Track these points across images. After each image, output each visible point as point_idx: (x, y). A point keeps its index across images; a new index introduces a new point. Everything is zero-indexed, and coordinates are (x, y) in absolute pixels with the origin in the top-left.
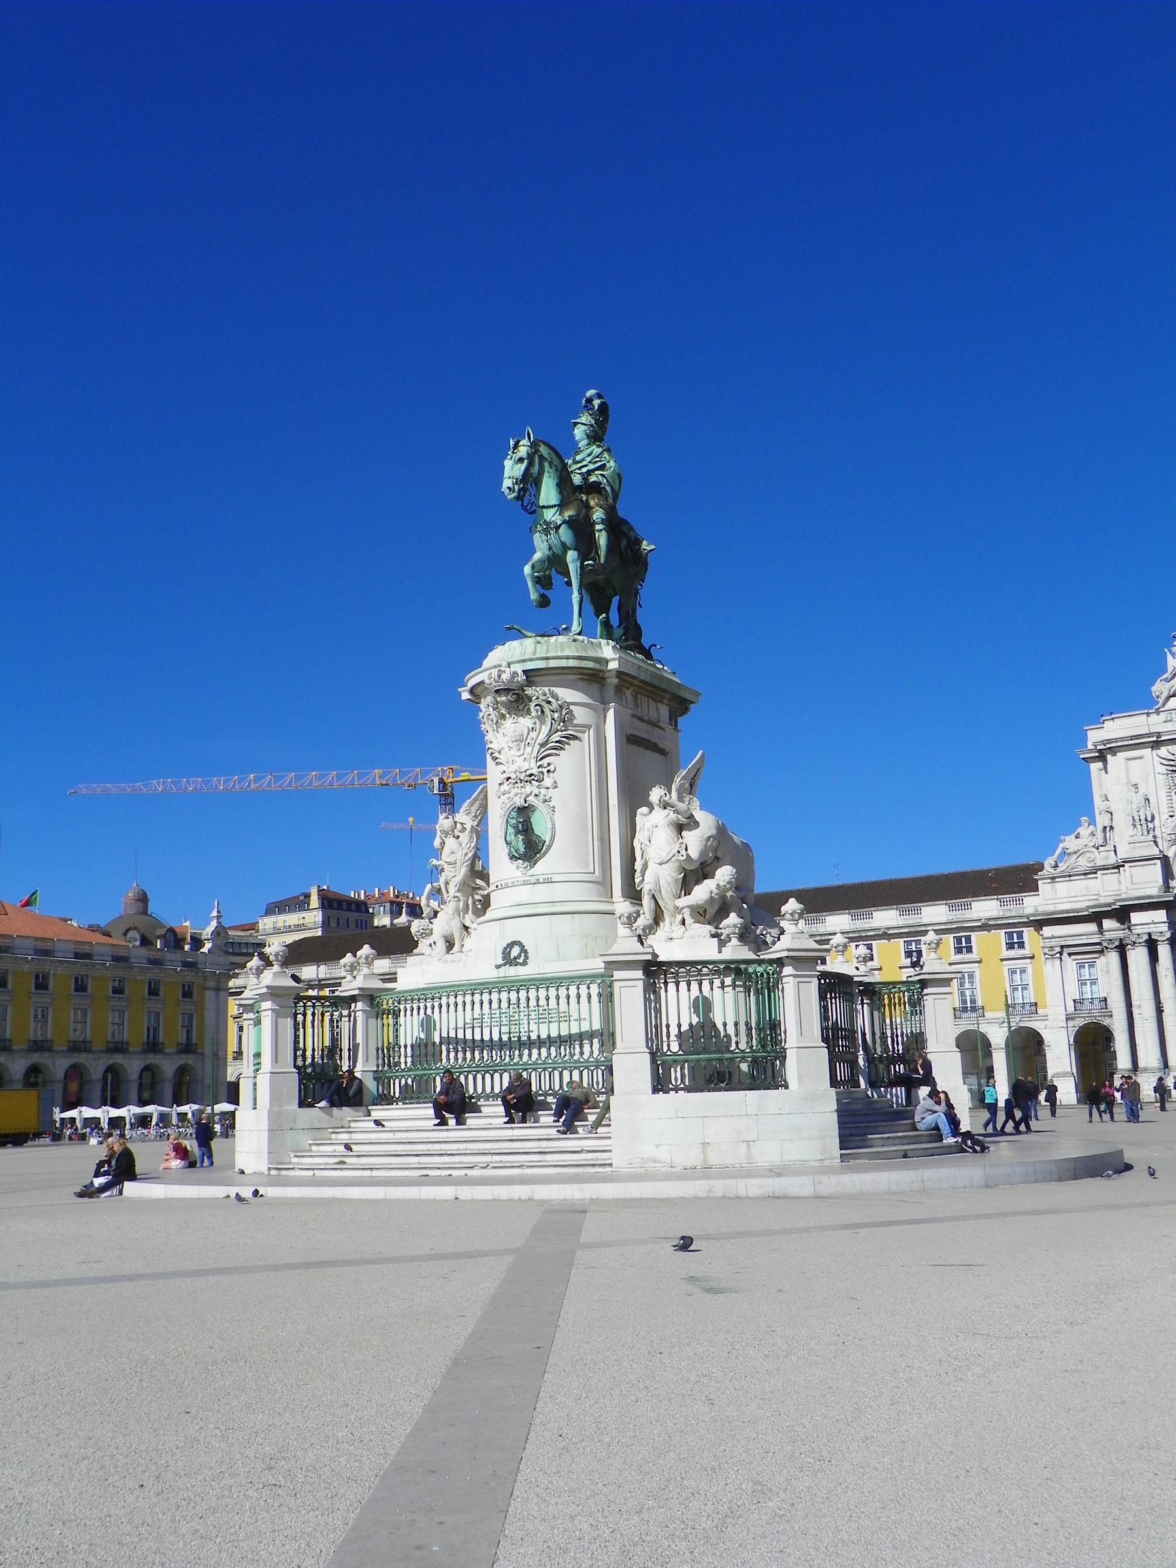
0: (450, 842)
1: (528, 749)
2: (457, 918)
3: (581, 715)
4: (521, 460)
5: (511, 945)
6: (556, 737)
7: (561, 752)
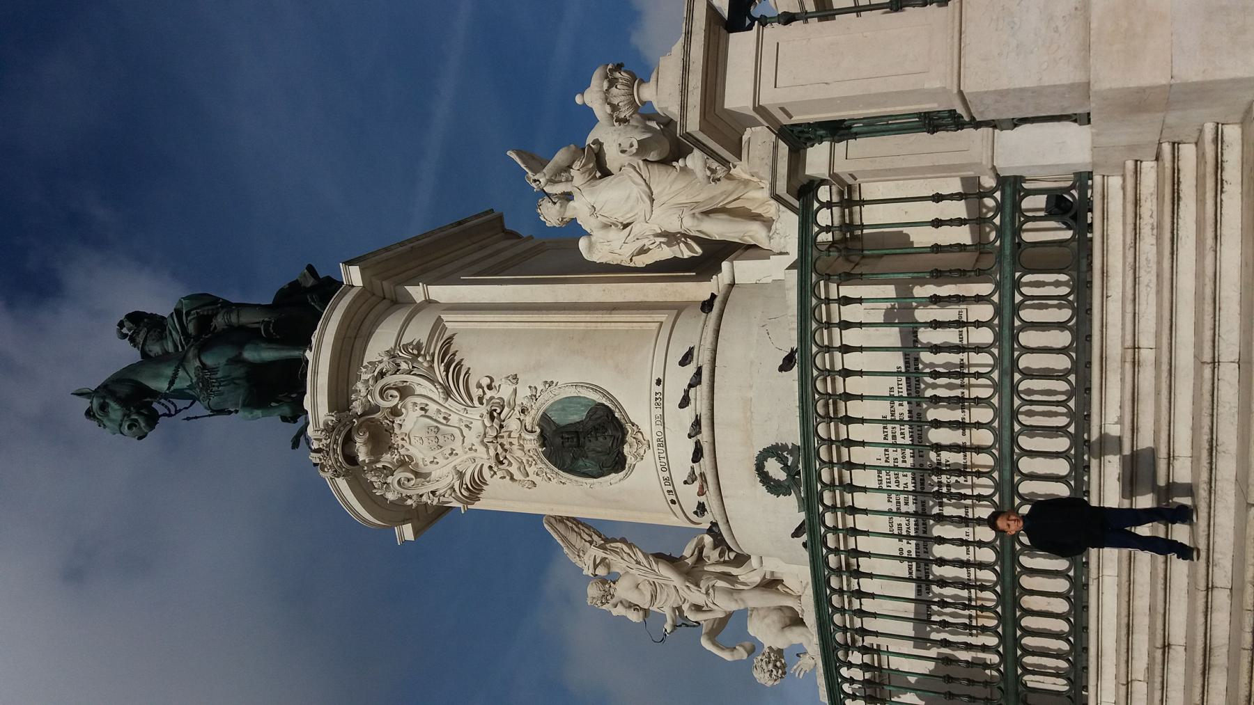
0: (622, 590)
1: (454, 419)
3: (419, 331)
5: (760, 469)
7: (466, 364)
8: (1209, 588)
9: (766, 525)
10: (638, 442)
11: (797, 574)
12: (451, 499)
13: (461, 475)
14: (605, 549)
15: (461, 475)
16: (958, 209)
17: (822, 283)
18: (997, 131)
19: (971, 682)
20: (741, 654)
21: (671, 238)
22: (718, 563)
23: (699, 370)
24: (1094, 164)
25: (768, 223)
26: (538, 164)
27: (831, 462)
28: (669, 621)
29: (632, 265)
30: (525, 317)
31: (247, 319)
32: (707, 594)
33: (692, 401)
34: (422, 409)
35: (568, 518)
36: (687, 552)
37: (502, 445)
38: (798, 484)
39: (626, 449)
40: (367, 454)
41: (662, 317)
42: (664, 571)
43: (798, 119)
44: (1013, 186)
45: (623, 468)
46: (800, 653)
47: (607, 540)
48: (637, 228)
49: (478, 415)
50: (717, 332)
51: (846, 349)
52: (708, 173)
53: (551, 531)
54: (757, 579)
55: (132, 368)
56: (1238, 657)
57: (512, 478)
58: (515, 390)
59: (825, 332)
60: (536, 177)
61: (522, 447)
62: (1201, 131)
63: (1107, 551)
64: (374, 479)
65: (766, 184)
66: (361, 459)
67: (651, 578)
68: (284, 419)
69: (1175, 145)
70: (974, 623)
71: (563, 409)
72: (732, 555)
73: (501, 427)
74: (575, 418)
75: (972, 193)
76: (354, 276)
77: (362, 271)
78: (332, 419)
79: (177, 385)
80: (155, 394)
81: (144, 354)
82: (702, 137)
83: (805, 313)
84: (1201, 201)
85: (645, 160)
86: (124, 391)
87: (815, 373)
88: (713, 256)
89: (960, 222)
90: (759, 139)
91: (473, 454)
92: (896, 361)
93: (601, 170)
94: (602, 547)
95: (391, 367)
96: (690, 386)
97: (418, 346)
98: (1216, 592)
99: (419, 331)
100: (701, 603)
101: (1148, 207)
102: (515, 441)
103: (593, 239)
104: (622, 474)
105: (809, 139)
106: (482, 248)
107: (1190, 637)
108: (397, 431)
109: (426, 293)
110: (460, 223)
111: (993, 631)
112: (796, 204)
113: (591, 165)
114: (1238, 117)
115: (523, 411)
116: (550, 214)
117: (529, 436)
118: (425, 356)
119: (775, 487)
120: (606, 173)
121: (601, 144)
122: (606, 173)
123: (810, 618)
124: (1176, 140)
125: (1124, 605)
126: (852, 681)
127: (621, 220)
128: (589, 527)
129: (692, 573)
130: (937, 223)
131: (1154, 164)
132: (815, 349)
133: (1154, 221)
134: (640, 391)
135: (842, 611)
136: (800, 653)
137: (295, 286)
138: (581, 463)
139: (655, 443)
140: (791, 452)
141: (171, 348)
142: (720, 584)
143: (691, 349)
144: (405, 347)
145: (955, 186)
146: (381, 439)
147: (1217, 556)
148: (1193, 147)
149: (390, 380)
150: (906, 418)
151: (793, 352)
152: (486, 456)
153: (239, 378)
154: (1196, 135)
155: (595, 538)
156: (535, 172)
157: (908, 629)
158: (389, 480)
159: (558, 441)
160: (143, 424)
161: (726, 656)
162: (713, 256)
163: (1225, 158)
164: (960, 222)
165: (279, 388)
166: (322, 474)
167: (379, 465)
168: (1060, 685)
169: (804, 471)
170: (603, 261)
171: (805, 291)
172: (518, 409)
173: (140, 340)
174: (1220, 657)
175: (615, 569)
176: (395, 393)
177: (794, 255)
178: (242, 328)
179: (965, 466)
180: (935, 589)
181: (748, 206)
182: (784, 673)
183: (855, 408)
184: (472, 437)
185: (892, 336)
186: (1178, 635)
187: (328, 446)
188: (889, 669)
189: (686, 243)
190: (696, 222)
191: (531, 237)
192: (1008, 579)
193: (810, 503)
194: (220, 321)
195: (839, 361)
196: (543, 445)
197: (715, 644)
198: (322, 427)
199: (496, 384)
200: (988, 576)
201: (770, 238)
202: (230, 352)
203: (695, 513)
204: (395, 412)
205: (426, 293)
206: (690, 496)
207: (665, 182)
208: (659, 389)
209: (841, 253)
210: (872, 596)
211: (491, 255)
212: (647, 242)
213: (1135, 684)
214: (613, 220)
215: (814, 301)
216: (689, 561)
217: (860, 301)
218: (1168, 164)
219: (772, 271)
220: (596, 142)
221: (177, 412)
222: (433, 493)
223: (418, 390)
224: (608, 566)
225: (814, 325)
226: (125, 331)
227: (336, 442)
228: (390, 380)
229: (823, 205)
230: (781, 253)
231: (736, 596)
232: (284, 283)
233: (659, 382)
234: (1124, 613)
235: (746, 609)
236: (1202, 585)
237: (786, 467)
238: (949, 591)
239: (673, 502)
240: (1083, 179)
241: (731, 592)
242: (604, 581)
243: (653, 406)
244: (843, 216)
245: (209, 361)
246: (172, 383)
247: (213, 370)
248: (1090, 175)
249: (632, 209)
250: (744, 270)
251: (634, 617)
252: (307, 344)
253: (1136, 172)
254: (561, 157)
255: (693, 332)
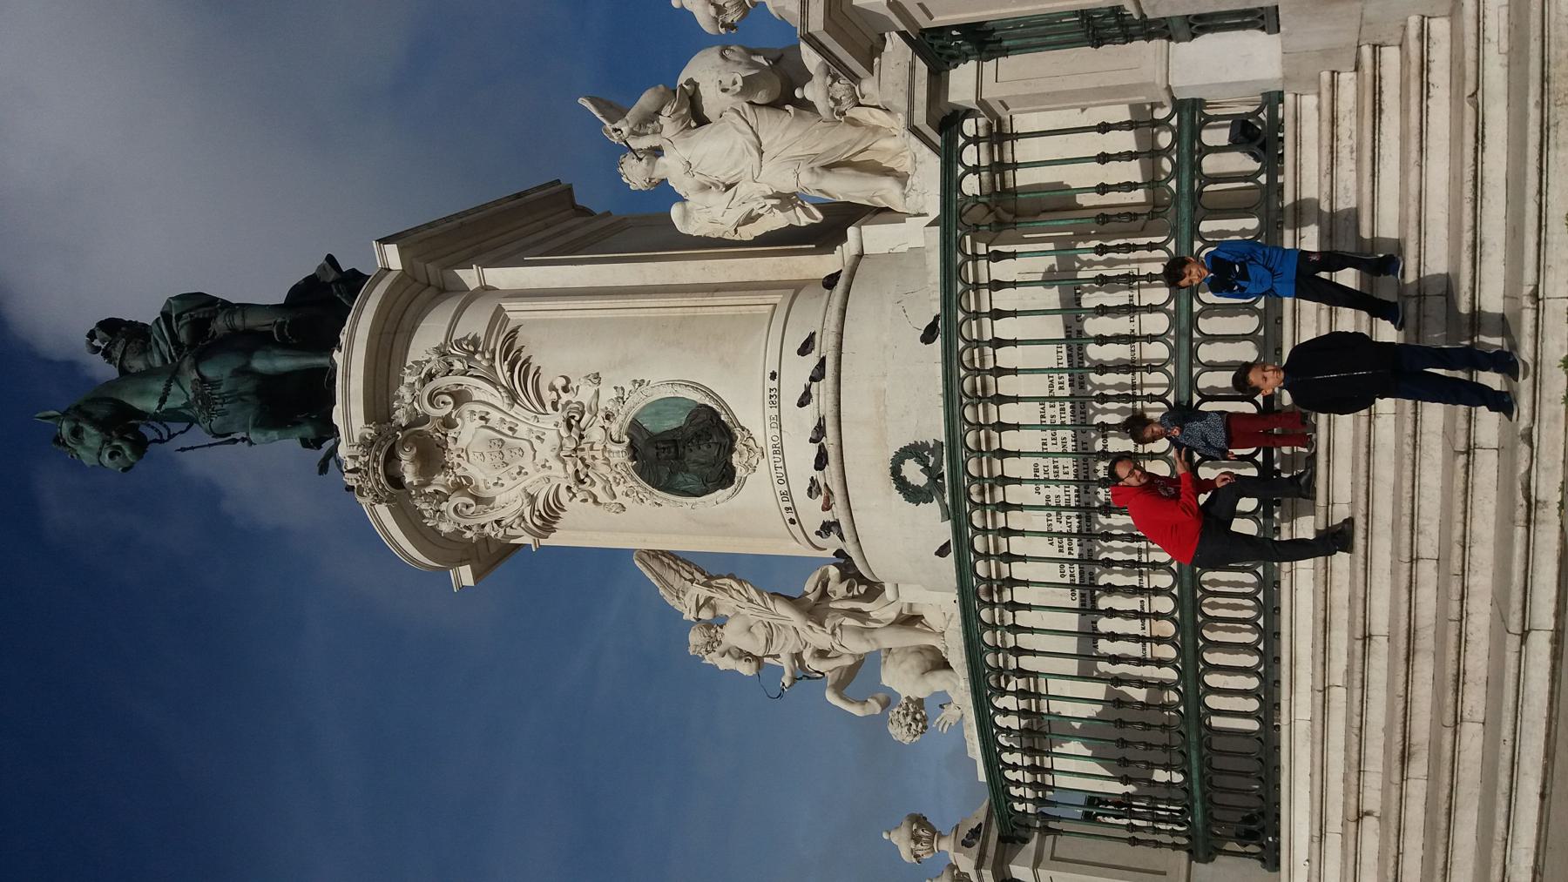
0: (732, 635)
1: (522, 430)
2: (877, 634)
4: (76, 432)
5: (896, 472)
6: (502, 371)
7: (535, 363)
8: (1414, 560)
9: (905, 543)
10: (750, 449)
11: (941, 607)
12: (520, 531)
13: (532, 499)
14: (710, 586)
15: (532, 499)
16: (1125, 141)
17: (968, 238)
18: (1172, 44)
19: (1147, 726)
20: (874, 707)
21: (786, 200)
22: (845, 598)
23: (823, 361)
24: (1286, 79)
25: (902, 179)
26: (615, 111)
27: (981, 477)
28: (788, 673)
29: (737, 238)
30: (606, 303)
31: (252, 321)
32: (833, 634)
33: (815, 397)
34: (482, 418)
35: (664, 553)
36: (809, 587)
37: (583, 460)
38: (941, 489)
39: (735, 458)
40: (415, 474)
41: (776, 298)
42: (782, 609)
43: (940, 20)
44: (1192, 112)
45: (732, 483)
46: (943, 701)
47: (710, 578)
48: (743, 189)
49: (551, 423)
50: (843, 312)
51: (997, 314)
52: (832, 104)
53: (643, 569)
54: (893, 615)
55: (110, 384)
56: (1445, 629)
57: (595, 501)
58: (597, 392)
59: (972, 293)
60: (616, 126)
61: (607, 461)
62: (1405, 28)
63: (1301, 564)
64: (424, 506)
65: (902, 118)
66: (407, 480)
67: (766, 618)
68: (305, 443)
69: (1376, 48)
70: (1144, 559)
71: (657, 413)
72: (863, 589)
73: (581, 437)
74: (671, 424)
75: (1142, 122)
76: (393, 257)
77: (401, 250)
78: (370, 432)
79: (169, 404)
80: (142, 415)
81: (123, 371)
82: (826, 39)
83: (950, 272)
84: (1404, 111)
85: (751, 103)
86: (102, 411)
87: (963, 373)
88: (837, 221)
89: (1130, 156)
90: (896, 50)
91: (546, 472)
92: (1054, 327)
93: (697, 117)
94: (707, 585)
95: (442, 366)
96: (812, 379)
97: (475, 341)
98: (1421, 564)
99: (474, 323)
100: (826, 646)
101: (1346, 126)
102: (599, 455)
103: (689, 205)
104: (730, 490)
105: (952, 57)
106: (547, 227)
107: (1393, 623)
108: (451, 446)
109: (481, 278)
110: (518, 196)
111: (1165, 567)
112: (937, 140)
113: (684, 111)
114: (1445, 8)
115: (607, 417)
116: (635, 174)
117: (615, 448)
118: (483, 353)
119: (913, 494)
120: (702, 121)
121: (696, 85)
122: (702, 121)
123: (957, 658)
124: (1377, 41)
125: (1321, 597)
126: (1008, 730)
127: (722, 179)
128: (689, 564)
129: (815, 610)
130: (1103, 158)
131: (1353, 75)
132: (961, 316)
133: (1354, 142)
134: (750, 386)
135: (993, 627)
136: (943, 701)
137: (311, 281)
138: (680, 478)
139: (770, 450)
140: (932, 452)
141: (157, 362)
142: (849, 622)
143: (812, 335)
144: (459, 343)
145: (1122, 114)
146: (432, 456)
147: (1422, 522)
148: (1397, 49)
149: (441, 382)
150: (1065, 365)
151: (937, 318)
152: (562, 474)
153: (246, 393)
154: (1399, 34)
155: (697, 575)
156: (613, 123)
157: (1071, 645)
158: (444, 506)
159: (652, 452)
160: (128, 453)
161: (856, 710)
162: (837, 221)
163: (1432, 57)
164: (1130, 156)
165: (302, 404)
166: (359, 499)
167: (429, 490)
168: (1253, 725)
169: (952, 474)
170: (701, 233)
171: (949, 247)
172: (601, 414)
173: (117, 354)
174: (1426, 641)
175: (722, 612)
176: (448, 399)
177: (934, 211)
178: (250, 333)
179: (1133, 361)
180: (1095, 378)
181: (878, 158)
182: (925, 727)
183: (1006, 385)
184: (545, 451)
185: (1051, 297)
186: (1380, 624)
187: (366, 464)
188: (1049, 713)
189: (803, 207)
190: (815, 179)
191: (608, 214)
192: (1187, 578)
193: (957, 516)
194: (220, 325)
195: (990, 328)
196: (633, 458)
197: (842, 697)
198: (357, 440)
199: (573, 385)
200: (1164, 580)
201: (905, 196)
202: (236, 361)
203: (818, 533)
204: (448, 423)
205: (481, 278)
206: (812, 513)
207: (780, 131)
208: (774, 384)
209: (988, 213)
210: (1029, 607)
211: (560, 234)
212: (755, 206)
213: (1333, 690)
214: (714, 179)
215: (960, 258)
216: (812, 597)
217: (1014, 255)
218: (1368, 70)
219: (911, 237)
220: (690, 82)
221: (171, 437)
222: (498, 522)
223: (477, 395)
224: (714, 608)
225: (960, 287)
226: (96, 343)
227: (376, 459)
228: (441, 382)
229: (969, 141)
230: (919, 215)
231: (867, 635)
232: (298, 277)
233: (773, 376)
234: (1321, 606)
235: (879, 651)
236: (1406, 556)
237: (926, 469)
238: (1111, 378)
239: (792, 521)
240: (1273, 99)
241: (861, 631)
242: (709, 625)
243: (767, 405)
244: (993, 182)
245: (210, 372)
246: (163, 401)
247: (215, 384)
248: (1279, 97)
249: (736, 165)
250: (873, 237)
251: (746, 669)
252: (334, 343)
253: (1333, 85)
254: (647, 100)
255: (813, 316)
